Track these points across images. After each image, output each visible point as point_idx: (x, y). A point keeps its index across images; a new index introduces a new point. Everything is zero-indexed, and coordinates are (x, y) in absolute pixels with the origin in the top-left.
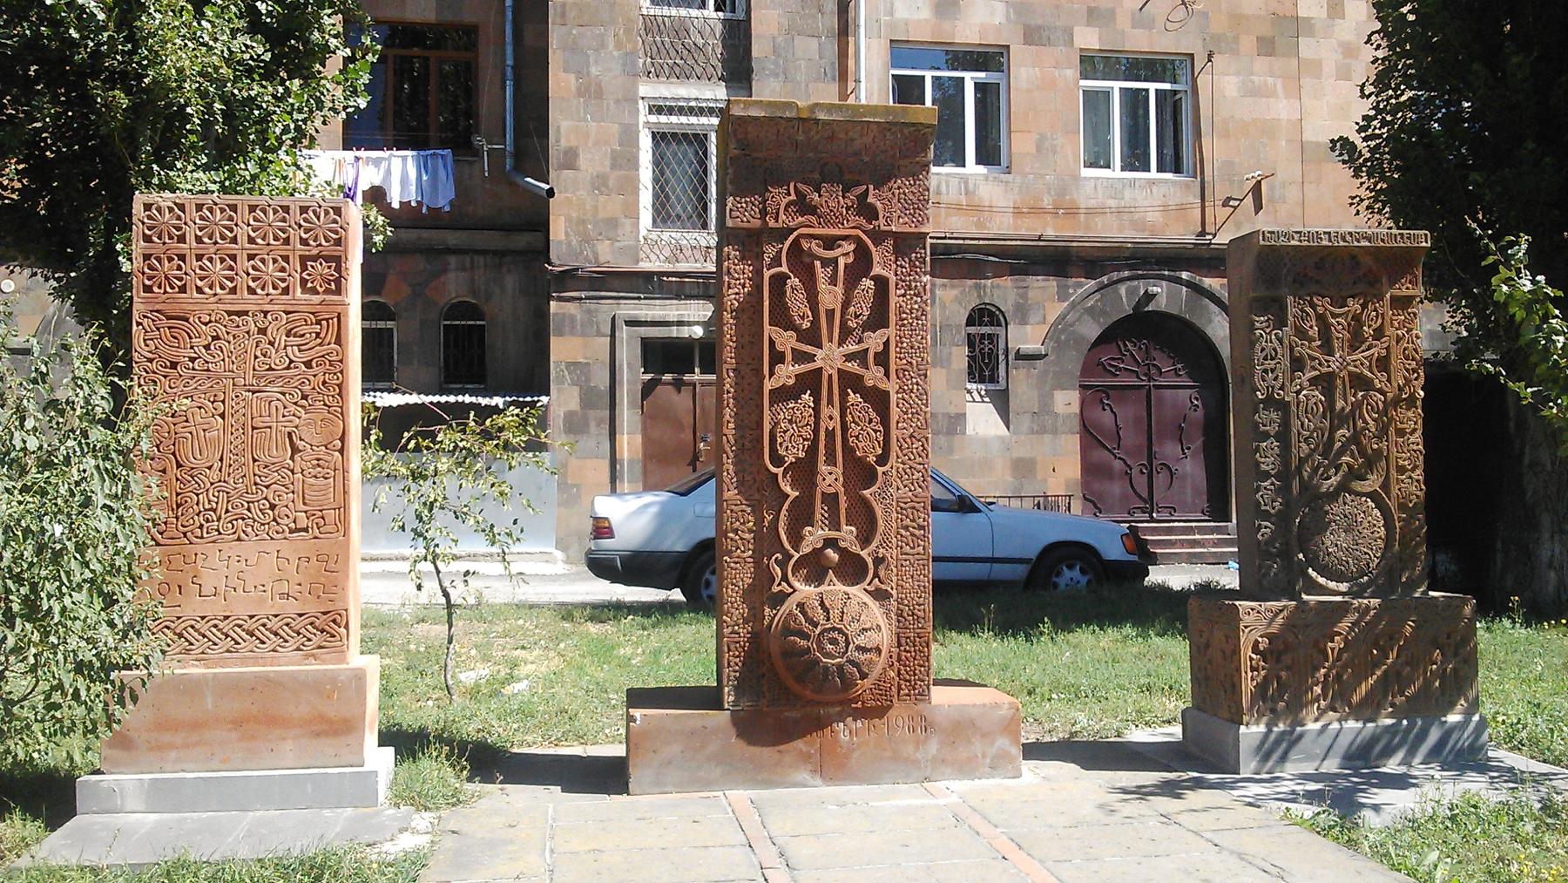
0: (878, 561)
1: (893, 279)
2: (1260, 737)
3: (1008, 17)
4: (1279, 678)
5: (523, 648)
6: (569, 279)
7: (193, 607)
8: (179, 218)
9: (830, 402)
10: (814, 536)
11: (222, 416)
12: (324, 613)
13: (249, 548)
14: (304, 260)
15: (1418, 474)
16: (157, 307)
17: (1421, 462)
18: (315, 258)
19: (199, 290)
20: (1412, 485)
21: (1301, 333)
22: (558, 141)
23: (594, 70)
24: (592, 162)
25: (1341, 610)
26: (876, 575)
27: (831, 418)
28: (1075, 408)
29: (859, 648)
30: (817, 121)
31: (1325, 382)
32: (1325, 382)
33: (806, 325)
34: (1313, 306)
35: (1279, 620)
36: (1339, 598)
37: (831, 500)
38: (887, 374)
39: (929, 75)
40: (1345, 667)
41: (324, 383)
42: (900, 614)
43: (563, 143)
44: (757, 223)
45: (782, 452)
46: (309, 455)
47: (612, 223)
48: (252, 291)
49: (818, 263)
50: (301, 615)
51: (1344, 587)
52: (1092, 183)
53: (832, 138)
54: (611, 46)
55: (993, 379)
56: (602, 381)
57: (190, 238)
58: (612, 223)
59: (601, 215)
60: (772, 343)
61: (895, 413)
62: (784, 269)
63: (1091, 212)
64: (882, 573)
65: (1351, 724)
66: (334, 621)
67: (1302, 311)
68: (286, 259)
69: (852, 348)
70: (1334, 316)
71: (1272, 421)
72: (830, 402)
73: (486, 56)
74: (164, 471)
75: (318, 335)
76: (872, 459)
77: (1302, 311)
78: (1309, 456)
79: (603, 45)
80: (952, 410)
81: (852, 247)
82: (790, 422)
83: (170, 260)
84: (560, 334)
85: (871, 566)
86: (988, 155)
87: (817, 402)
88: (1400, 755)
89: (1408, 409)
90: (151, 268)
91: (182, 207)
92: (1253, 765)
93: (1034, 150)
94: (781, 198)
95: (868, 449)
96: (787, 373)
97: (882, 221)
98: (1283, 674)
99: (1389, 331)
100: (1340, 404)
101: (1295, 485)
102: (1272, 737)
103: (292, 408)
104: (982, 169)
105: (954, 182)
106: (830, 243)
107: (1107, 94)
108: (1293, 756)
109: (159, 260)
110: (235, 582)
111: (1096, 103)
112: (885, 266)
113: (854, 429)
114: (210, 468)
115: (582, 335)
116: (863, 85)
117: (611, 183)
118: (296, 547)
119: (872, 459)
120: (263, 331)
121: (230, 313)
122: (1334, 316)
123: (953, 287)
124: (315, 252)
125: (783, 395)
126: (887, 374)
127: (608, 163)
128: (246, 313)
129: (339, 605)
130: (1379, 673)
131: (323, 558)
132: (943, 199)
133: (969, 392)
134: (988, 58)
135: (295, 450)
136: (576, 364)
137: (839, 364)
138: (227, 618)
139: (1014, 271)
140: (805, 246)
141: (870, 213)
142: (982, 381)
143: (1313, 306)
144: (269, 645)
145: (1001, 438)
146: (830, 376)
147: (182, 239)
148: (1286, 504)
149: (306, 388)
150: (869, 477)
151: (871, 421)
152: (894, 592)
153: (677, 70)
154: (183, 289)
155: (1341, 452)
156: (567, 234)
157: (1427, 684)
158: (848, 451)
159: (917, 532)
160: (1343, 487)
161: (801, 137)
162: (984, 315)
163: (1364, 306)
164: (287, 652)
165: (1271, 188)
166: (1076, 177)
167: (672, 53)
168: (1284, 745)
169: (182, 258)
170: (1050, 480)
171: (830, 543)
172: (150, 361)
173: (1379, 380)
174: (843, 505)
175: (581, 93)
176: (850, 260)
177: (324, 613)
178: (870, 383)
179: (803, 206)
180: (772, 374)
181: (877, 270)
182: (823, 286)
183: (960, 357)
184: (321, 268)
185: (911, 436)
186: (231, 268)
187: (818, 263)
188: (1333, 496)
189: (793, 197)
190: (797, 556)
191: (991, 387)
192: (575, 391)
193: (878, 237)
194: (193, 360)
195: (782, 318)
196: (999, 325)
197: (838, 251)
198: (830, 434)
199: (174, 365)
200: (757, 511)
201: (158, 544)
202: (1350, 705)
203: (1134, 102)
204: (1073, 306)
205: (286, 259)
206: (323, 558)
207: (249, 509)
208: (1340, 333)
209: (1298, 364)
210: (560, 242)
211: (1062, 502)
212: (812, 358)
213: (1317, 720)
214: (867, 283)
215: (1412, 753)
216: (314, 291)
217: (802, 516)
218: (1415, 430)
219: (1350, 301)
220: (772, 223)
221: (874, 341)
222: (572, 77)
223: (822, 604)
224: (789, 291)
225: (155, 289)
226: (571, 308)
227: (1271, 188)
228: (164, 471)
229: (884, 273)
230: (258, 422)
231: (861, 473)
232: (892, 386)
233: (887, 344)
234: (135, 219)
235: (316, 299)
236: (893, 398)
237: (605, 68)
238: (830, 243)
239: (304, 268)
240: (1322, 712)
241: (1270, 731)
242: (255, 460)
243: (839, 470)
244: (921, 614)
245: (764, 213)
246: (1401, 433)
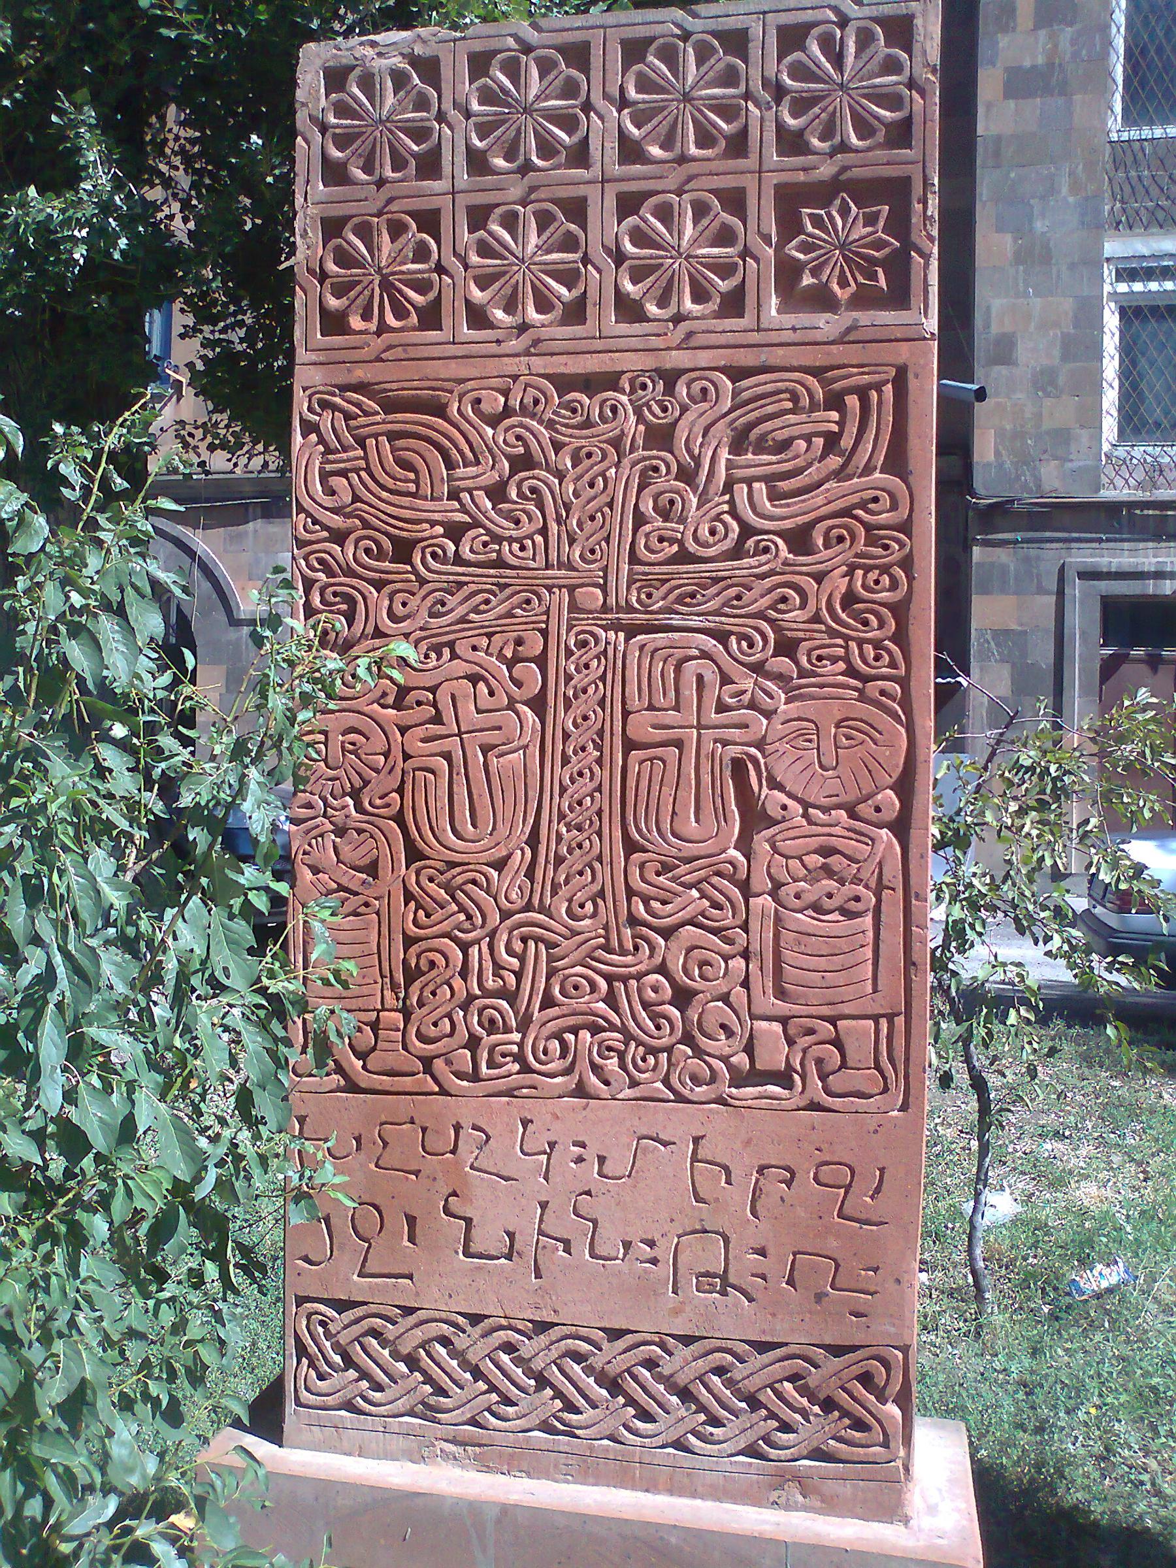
5: (1058, 1135)
6: (999, 514)
7: (447, 1284)
8: (422, 104)
11: (538, 704)
12: (837, 1351)
13: (610, 1123)
14: (790, 201)
16: (360, 374)
18: (823, 193)
19: (478, 317)
22: (987, 326)
23: (1039, 226)
24: (1035, 351)
41: (850, 599)
43: (995, 329)
46: (797, 834)
47: (1062, 437)
48: (629, 310)
50: (762, 1347)
54: (1065, 190)
56: (1044, 655)
57: (454, 162)
58: (1062, 437)
59: (1046, 426)
66: (866, 1379)
68: (735, 201)
74: (372, 869)
75: (832, 441)
79: (1053, 190)
83: (397, 230)
84: (985, 591)
90: (345, 259)
91: (429, 68)
103: (747, 683)
109: (365, 232)
110: (563, 1223)
114: (500, 865)
115: (1015, 593)
117: (1061, 380)
118: (761, 1127)
120: (660, 437)
121: (563, 383)
124: (826, 170)
127: (1057, 353)
128: (611, 381)
129: (881, 1331)
131: (839, 1178)
135: (754, 818)
136: (1007, 632)
138: (542, 1327)
144: (663, 1427)
147: (430, 166)
149: (795, 616)
153: (1161, 215)
156: (997, 453)
164: (722, 1455)
167: (1154, 191)
169: (429, 221)
172: (339, 537)
175: (1019, 258)
177: (837, 1351)
184: (852, 226)
186: (569, 243)
192: (1005, 671)
194: (455, 532)
199: (403, 550)
201: (352, 1087)
206: (839, 1178)
207: (611, 1000)
210: (989, 464)
216: (822, 300)
222: (1009, 238)
225: (356, 322)
226: (1002, 555)
230: (642, 726)
234: (301, 117)
235: (826, 324)
237: (1055, 223)
239: (790, 226)
242: (631, 847)
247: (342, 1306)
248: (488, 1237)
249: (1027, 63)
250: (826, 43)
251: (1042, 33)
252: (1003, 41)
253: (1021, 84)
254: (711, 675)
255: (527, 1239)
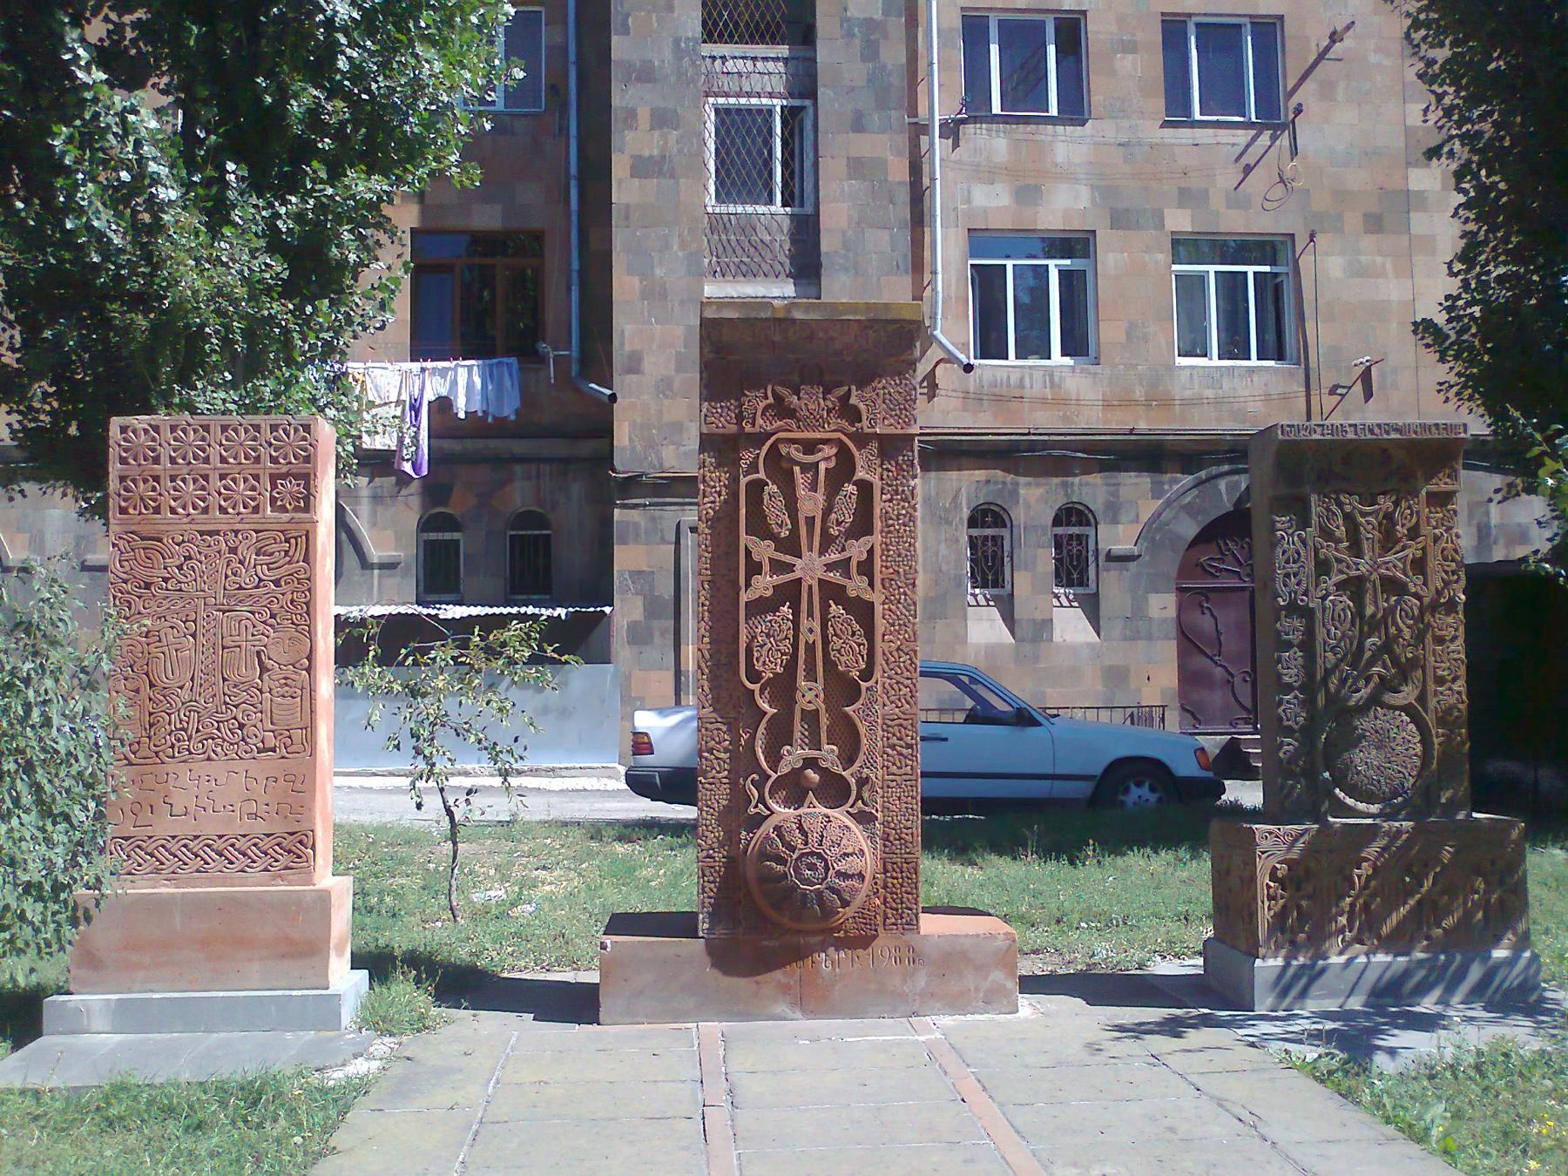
0: (862, 782)
1: (877, 484)
2: (1277, 972)
3: (1093, 201)
4: (1299, 908)
5: (544, 868)
6: (632, 485)
7: (164, 826)
8: (154, 440)
9: (810, 614)
10: (793, 756)
11: (194, 636)
12: (291, 834)
13: (218, 769)
14: (274, 478)
15: (1460, 686)
16: (133, 528)
17: (1462, 671)
18: (284, 476)
19: (173, 511)
20: (1454, 694)
21: (1327, 534)
22: (622, 344)
23: (658, 272)
25: (1371, 833)
26: (859, 797)
27: (811, 631)
28: (1172, 612)
29: (839, 874)
30: (794, 321)
31: (1354, 587)
32: (1354, 587)
33: (784, 533)
34: (1340, 505)
35: (1300, 844)
36: (1369, 821)
37: (811, 717)
38: (871, 585)
39: (1009, 264)
40: (1373, 896)
41: (292, 601)
42: (886, 838)
43: (627, 348)
44: (733, 429)
45: (759, 667)
46: (277, 673)
48: (223, 510)
49: (797, 469)
50: (268, 835)
51: (1374, 809)
52: (1188, 372)
53: (811, 337)
54: (675, 247)
55: (1082, 582)
56: (667, 591)
57: (165, 460)
59: (666, 419)
60: (748, 552)
61: (880, 625)
62: (762, 475)
63: (1189, 403)
64: (866, 795)
65: (1381, 958)
66: (301, 842)
67: (1328, 509)
68: (256, 477)
69: (834, 557)
70: (1364, 515)
71: (1295, 629)
72: (810, 614)
73: (552, 262)
74: (137, 691)
75: (286, 552)
76: (855, 674)
77: (1328, 509)
78: (1336, 666)
79: (667, 246)
80: (1039, 616)
81: (834, 450)
82: (768, 636)
83: (145, 481)
84: (624, 542)
85: (854, 787)
86: (1075, 344)
87: (796, 614)
88: (1436, 993)
89: (1448, 614)
90: (127, 489)
91: (156, 429)
92: (1270, 1001)
93: (1123, 339)
94: (758, 401)
95: (850, 662)
96: (765, 584)
97: (865, 423)
98: (1304, 903)
99: (1425, 530)
100: (1369, 610)
101: (1321, 700)
102: (1290, 972)
103: (261, 627)
104: (1068, 361)
105: (1038, 375)
106: (810, 447)
107: (1202, 278)
108: (1314, 990)
109: (134, 481)
110: (205, 802)
111: (1191, 288)
112: (870, 469)
113: (836, 643)
116: (940, 277)
117: (676, 386)
118: (268, 764)
119: (855, 674)
120: (233, 551)
121: (202, 533)
122: (1364, 515)
123: (1038, 485)
124: (284, 470)
125: (760, 607)
126: (871, 585)
127: (672, 366)
128: (217, 533)
129: (303, 826)
130: (1412, 902)
131: (291, 778)
132: (1027, 393)
133: (1057, 597)
134: (1074, 244)
135: (264, 669)
136: (640, 573)
137: (820, 574)
138: (197, 837)
139: (1104, 467)
140: (784, 450)
141: (854, 415)
142: (1070, 584)
143: (1340, 505)
144: (237, 866)
145: (1088, 644)
146: (810, 587)
147: (156, 460)
148: (1311, 719)
149: (275, 606)
150: (853, 694)
151: (854, 634)
152: (879, 815)
153: (744, 268)
154: (157, 510)
155: (1372, 662)
157: (1468, 915)
158: (830, 665)
159: (904, 751)
160: (1374, 700)
161: (777, 338)
162: (1072, 514)
163: (1397, 504)
164: (255, 873)
165: (1382, 375)
166: (1171, 367)
167: (739, 251)
168: (1303, 981)
169: (156, 479)
170: (1145, 690)
171: (810, 763)
172: (125, 582)
173: (1414, 583)
174: (824, 721)
175: (646, 294)
176: (832, 464)
177: (291, 834)
178: (852, 594)
179: (781, 410)
180: (748, 585)
181: (860, 474)
182: (802, 492)
183: (1046, 559)
184: (291, 486)
185: (898, 649)
186: (203, 488)
187: (797, 469)
188: (1362, 709)
189: (771, 400)
190: (774, 776)
191: (1080, 590)
193: (862, 440)
194: (166, 580)
195: (759, 527)
196: (1088, 524)
197: (819, 455)
198: (811, 648)
199: (148, 586)
200: (732, 728)
202: (1379, 938)
203: (1232, 287)
204: (1168, 503)
205: (256, 477)
206: (291, 778)
207: (218, 729)
208: (1370, 533)
209: (1323, 567)
210: (623, 449)
211: (1157, 713)
212: (790, 568)
213: (1341, 953)
214: (850, 488)
215: (1450, 990)
216: (283, 509)
217: (780, 735)
218: (1455, 638)
219: (1381, 499)
220: (748, 428)
221: (857, 550)
222: (636, 280)
223: (800, 828)
224: (766, 497)
225: (131, 511)
226: (635, 515)
227: (1382, 375)
228: (137, 691)
229: (868, 477)
231: (844, 689)
232: (877, 597)
233: (871, 552)
234: (111, 442)
235: (285, 517)
236: (879, 609)
237: (669, 270)
238: (810, 447)
239: (274, 486)
240: (1347, 945)
241: (1287, 965)
242: (224, 680)
243: (820, 686)
244: (909, 838)
245: (740, 418)
246: (1440, 641)
247: (126, 839)
248: (178, 810)
249: (647, 154)
250: (285, 430)
251: (657, 134)
252: (629, 136)
253: (642, 168)
254: (249, 624)
255: (192, 809)
